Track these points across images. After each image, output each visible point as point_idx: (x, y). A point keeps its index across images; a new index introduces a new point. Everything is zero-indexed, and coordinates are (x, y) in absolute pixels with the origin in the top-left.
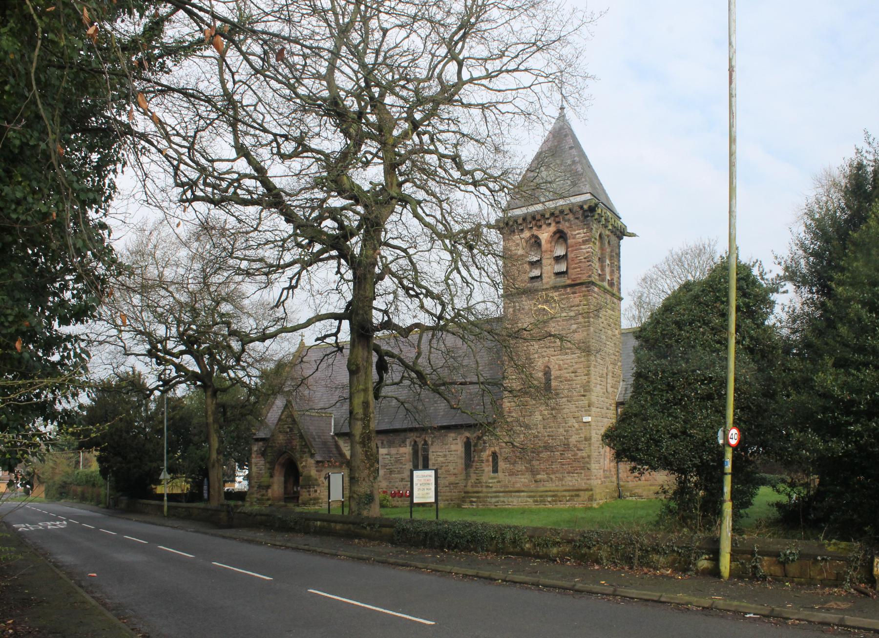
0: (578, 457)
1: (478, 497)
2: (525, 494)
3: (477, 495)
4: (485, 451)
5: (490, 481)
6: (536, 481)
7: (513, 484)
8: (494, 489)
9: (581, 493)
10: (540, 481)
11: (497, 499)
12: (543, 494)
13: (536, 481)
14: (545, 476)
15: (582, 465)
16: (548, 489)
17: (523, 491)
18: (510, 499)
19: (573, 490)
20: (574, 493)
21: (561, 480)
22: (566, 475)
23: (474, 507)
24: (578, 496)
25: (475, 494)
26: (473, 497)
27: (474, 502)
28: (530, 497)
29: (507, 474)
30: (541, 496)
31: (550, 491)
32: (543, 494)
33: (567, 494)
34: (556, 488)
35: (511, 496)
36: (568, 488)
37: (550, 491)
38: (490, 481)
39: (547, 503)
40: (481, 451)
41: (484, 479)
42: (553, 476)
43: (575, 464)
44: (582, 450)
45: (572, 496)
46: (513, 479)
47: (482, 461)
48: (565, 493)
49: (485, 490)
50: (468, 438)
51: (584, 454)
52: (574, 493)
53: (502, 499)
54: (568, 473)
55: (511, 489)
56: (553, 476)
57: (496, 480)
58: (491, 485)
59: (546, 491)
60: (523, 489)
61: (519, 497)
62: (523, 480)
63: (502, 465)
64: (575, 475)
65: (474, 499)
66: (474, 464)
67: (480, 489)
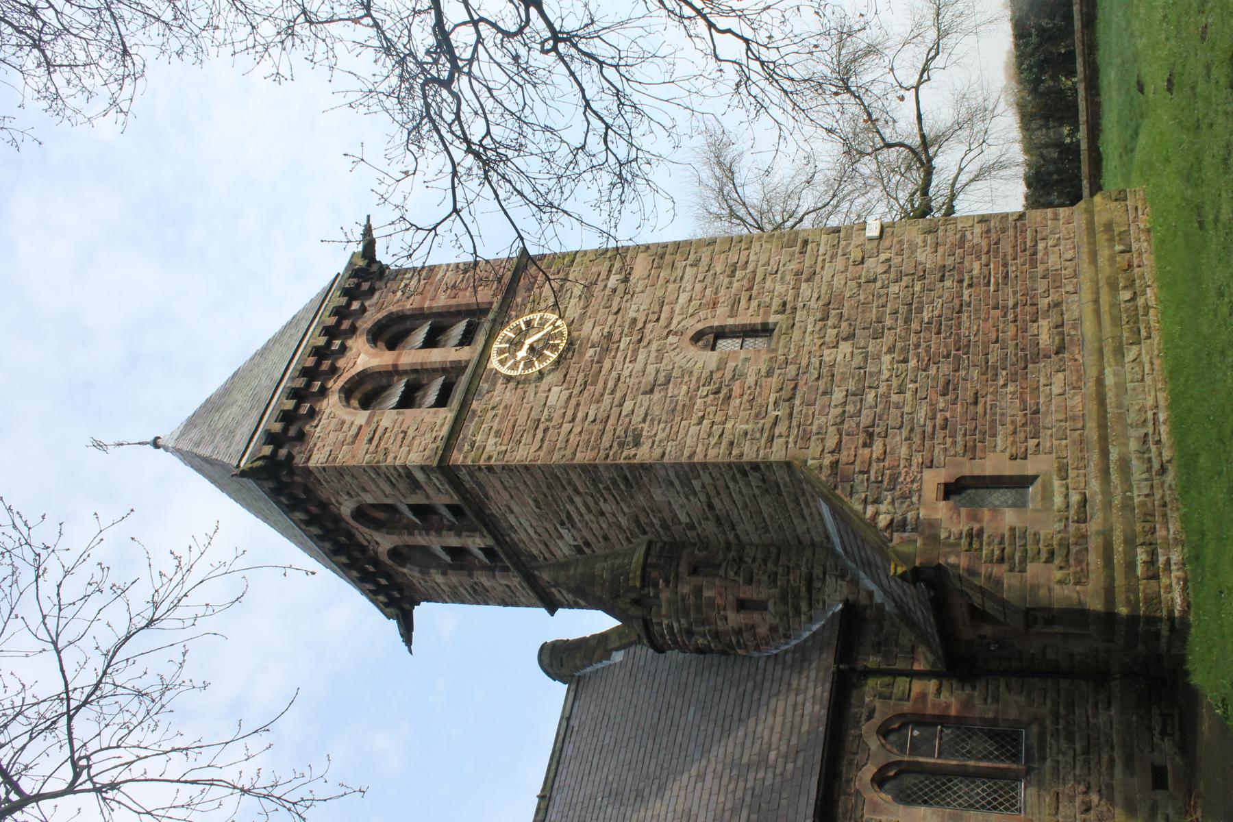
0: (984, 244)
1: (1130, 542)
2: (1108, 371)
3: (1119, 548)
4: (933, 524)
5: (1058, 500)
6: (1060, 350)
7: (1074, 418)
8: (1095, 485)
9: (1099, 220)
10: (1062, 333)
11: (1136, 465)
12: (1106, 318)
13: (1060, 350)
14: (1044, 324)
15: (1011, 232)
16: (1088, 309)
17: (1100, 382)
18: (1132, 417)
19: (1092, 243)
20: (1101, 238)
21: (1054, 280)
22: (1040, 269)
23: (1175, 557)
24: (1109, 227)
25: (1118, 559)
26: (1131, 565)
27: (1152, 562)
28: (1119, 352)
29: (1032, 443)
30: (1116, 321)
31: (1096, 301)
32: (1106, 318)
33: (1104, 254)
34: (1086, 287)
35: (1121, 417)
36: (1085, 256)
37: (1096, 301)
38: (1058, 500)
39: (1140, 301)
40: (934, 538)
41: (1050, 529)
42: (1043, 303)
43: (1006, 247)
44: (963, 237)
45: (1111, 239)
46: (1051, 419)
47: (975, 536)
48: (1102, 260)
49: (1094, 526)
50: (880, 781)
51: (978, 229)
52: (1101, 238)
53: (1133, 445)
54: (1034, 265)
55: (1092, 425)
56: (1043, 303)
57: (1057, 483)
58: (1075, 498)
59: (1097, 312)
60: (1091, 384)
61: (1121, 388)
62: (1056, 390)
63: (994, 463)
64: (1041, 245)
65: (1141, 556)
66: (983, 569)
67: (1094, 543)
